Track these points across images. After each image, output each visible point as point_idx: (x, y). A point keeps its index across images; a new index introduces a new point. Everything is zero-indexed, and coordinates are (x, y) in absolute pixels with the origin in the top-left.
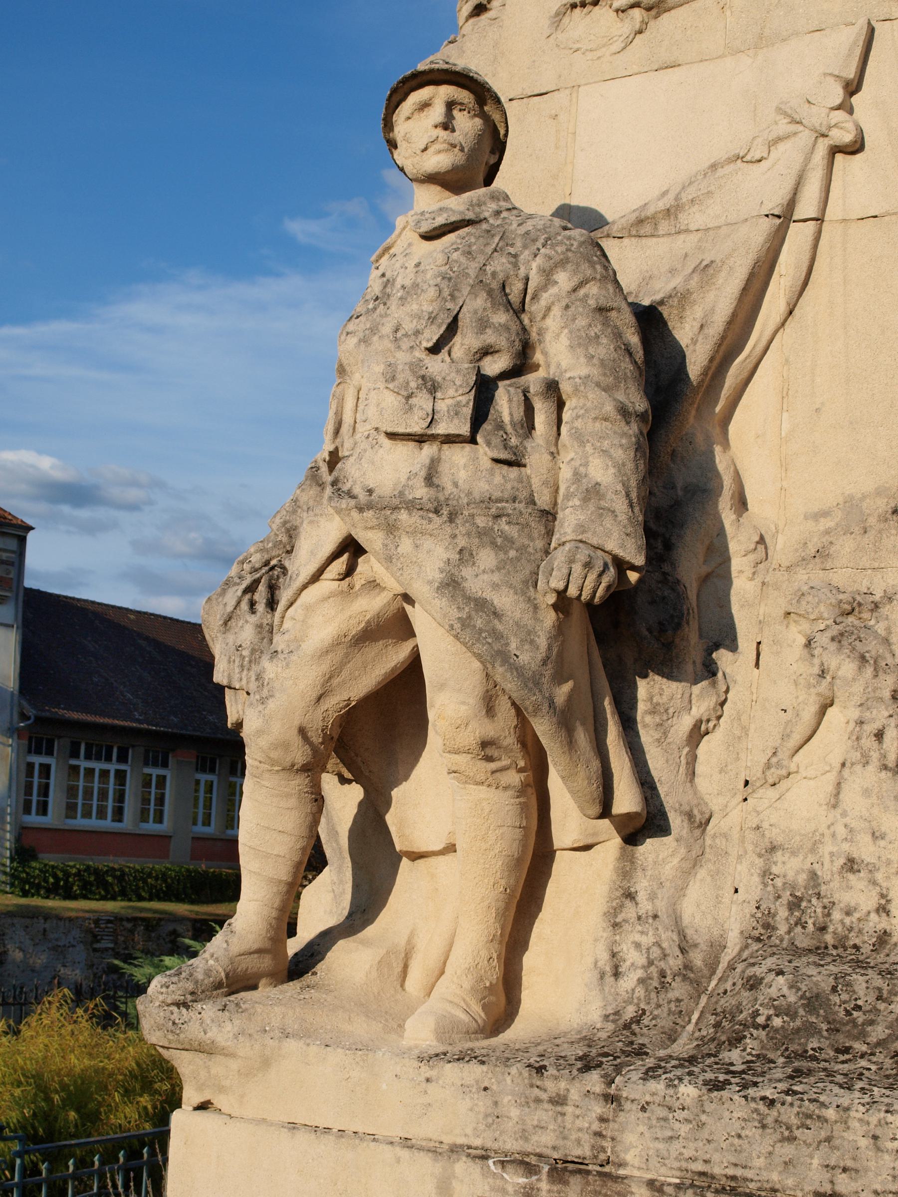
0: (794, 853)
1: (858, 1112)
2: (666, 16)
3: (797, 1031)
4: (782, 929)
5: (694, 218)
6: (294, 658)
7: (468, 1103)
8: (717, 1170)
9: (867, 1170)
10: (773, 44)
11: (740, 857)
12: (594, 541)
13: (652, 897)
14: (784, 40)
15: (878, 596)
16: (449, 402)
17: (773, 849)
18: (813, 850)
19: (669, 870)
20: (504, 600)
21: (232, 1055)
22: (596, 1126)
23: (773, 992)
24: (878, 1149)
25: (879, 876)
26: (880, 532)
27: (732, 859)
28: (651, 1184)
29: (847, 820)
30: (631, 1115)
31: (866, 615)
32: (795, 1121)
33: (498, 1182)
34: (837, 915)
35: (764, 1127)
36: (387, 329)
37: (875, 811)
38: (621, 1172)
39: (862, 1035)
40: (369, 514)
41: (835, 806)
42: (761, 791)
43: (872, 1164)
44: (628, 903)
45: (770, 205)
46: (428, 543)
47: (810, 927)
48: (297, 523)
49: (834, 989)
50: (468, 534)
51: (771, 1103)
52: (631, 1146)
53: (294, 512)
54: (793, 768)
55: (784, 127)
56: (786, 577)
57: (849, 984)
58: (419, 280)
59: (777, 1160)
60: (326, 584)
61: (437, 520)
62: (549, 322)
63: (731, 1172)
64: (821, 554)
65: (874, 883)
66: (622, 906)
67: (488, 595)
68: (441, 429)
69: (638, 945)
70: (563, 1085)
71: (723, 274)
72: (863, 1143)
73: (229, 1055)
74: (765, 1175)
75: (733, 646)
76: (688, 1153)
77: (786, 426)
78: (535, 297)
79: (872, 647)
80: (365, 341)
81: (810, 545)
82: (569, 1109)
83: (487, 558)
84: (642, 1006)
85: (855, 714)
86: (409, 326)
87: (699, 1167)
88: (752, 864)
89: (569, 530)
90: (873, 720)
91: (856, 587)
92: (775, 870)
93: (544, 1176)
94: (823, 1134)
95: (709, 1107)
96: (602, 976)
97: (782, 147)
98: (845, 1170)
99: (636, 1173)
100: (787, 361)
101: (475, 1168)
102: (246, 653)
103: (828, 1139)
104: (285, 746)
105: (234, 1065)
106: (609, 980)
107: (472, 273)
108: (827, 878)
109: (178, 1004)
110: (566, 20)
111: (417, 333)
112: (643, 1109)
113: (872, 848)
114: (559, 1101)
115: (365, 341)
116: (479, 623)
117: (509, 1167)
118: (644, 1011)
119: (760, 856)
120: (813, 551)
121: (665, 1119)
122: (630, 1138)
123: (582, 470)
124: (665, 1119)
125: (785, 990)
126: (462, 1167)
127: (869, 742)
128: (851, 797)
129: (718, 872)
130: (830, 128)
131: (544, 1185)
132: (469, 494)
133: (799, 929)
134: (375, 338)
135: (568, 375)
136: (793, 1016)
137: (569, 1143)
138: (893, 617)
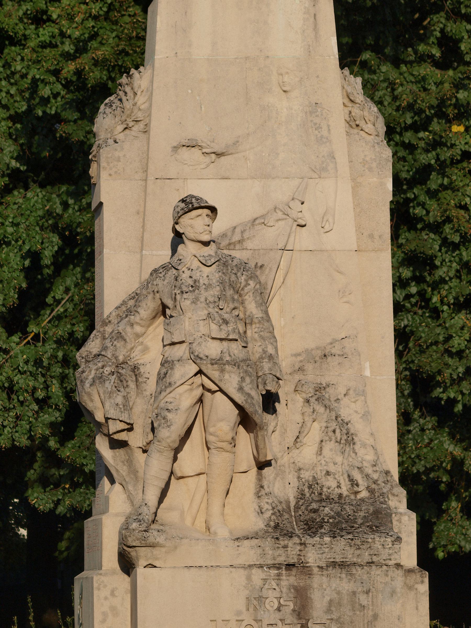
0: (307, 471)
1: (377, 539)
2: (223, 158)
3: (338, 523)
4: (308, 495)
5: (249, 244)
6: (179, 412)
7: (253, 551)
8: (337, 560)
9: (381, 554)
10: (268, 179)
11: (289, 473)
12: (274, 374)
13: (269, 487)
14: (273, 178)
15: (324, 385)
16: (231, 328)
17: (300, 469)
18: (313, 469)
19: (271, 478)
20: (253, 393)
21: (164, 546)
22: (298, 553)
23: (326, 512)
24: (384, 548)
25: (336, 476)
26: (321, 362)
27: (287, 473)
28: (318, 567)
29: (325, 459)
30: (310, 548)
31: (322, 391)
32: (360, 543)
33: (268, 573)
34: (325, 489)
35: (351, 546)
36: (202, 299)
37: (334, 456)
38: (307, 565)
39: (356, 523)
40: (216, 366)
41: (320, 455)
42: (294, 451)
43: (383, 552)
44: (262, 489)
45: (281, 246)
46: (233, 376)
47: (316, 494)
48: (118, 355)
49: (341, 510)
50: (243, 372)
51: (352, 540)
52: (310, 557)
53: (116, 350)
54: (304, 442)
55: (280, 215)
56: (291, 377)
57: (345, 509)
58: (211, 283)
59: (355, 555)
60: (185, 387)
61: (236, 368)
62: (247, 297)
63: (341, 560)
64: (301, 369)
65: (335, 479)
66: (260, 490)
67: (250, 392)
68: (231, 337)
69: (267, 503)
70: (286, 542)
71: (268, 270)
72: (380, 547)
73: (162, 546)
74: (352, 560)
75: (279, 402)
76: (328, 557)
77: (283, 323)
78: (243, 289)
79: (327, 402)
80: (193, 302)
81: (296, 366)
82: (289, 549)
83: (248, 380)
84: (276, 521)
85: (325, 424)
86: (211, 299)
87: (332, 560)
88: (294, 475)
89: (267, 370)
90: (331, 426)
91: (316, 382)
92: (301, 476)
93: (284, 569)
94: (368, 546)
95: (334, 543)
96: (258, 513)
97: (280, 223)
98: (375, 555)
99: (312, 565)
100: (282, 299)
101: (260, 571)
102: (121, 406)
103: (370, 547)
104: (174, 441)
105: (163, 550)
106: (261, 515)
107: (227, 281)
108: (320, 477)
109: (145, 531)
110: (179, 150)
111: (215, 302)
112: (313, 546)
113: (334, 468)
114: (285, 547)
115: (193, 302)
116: (249, 401)
117: (271, 569)
118: (278, 523)
119: (296, 472)
120: (297, 368)
121: (321, 548)
122: (310, 555)
123: (265, 349)
124: (321, 548)
125: (330, 511)
126: (254, 571)
127: (331, 434)
128: (326, 451)
129: (283, 478)
130: (298, 219)
131: (284, 572)
132: (239, 358)
133: (313, 495)
134: (199, 302)
135: (256, 316)
136: (335, 519)
137: (289, 559)
138: (330, 392)
